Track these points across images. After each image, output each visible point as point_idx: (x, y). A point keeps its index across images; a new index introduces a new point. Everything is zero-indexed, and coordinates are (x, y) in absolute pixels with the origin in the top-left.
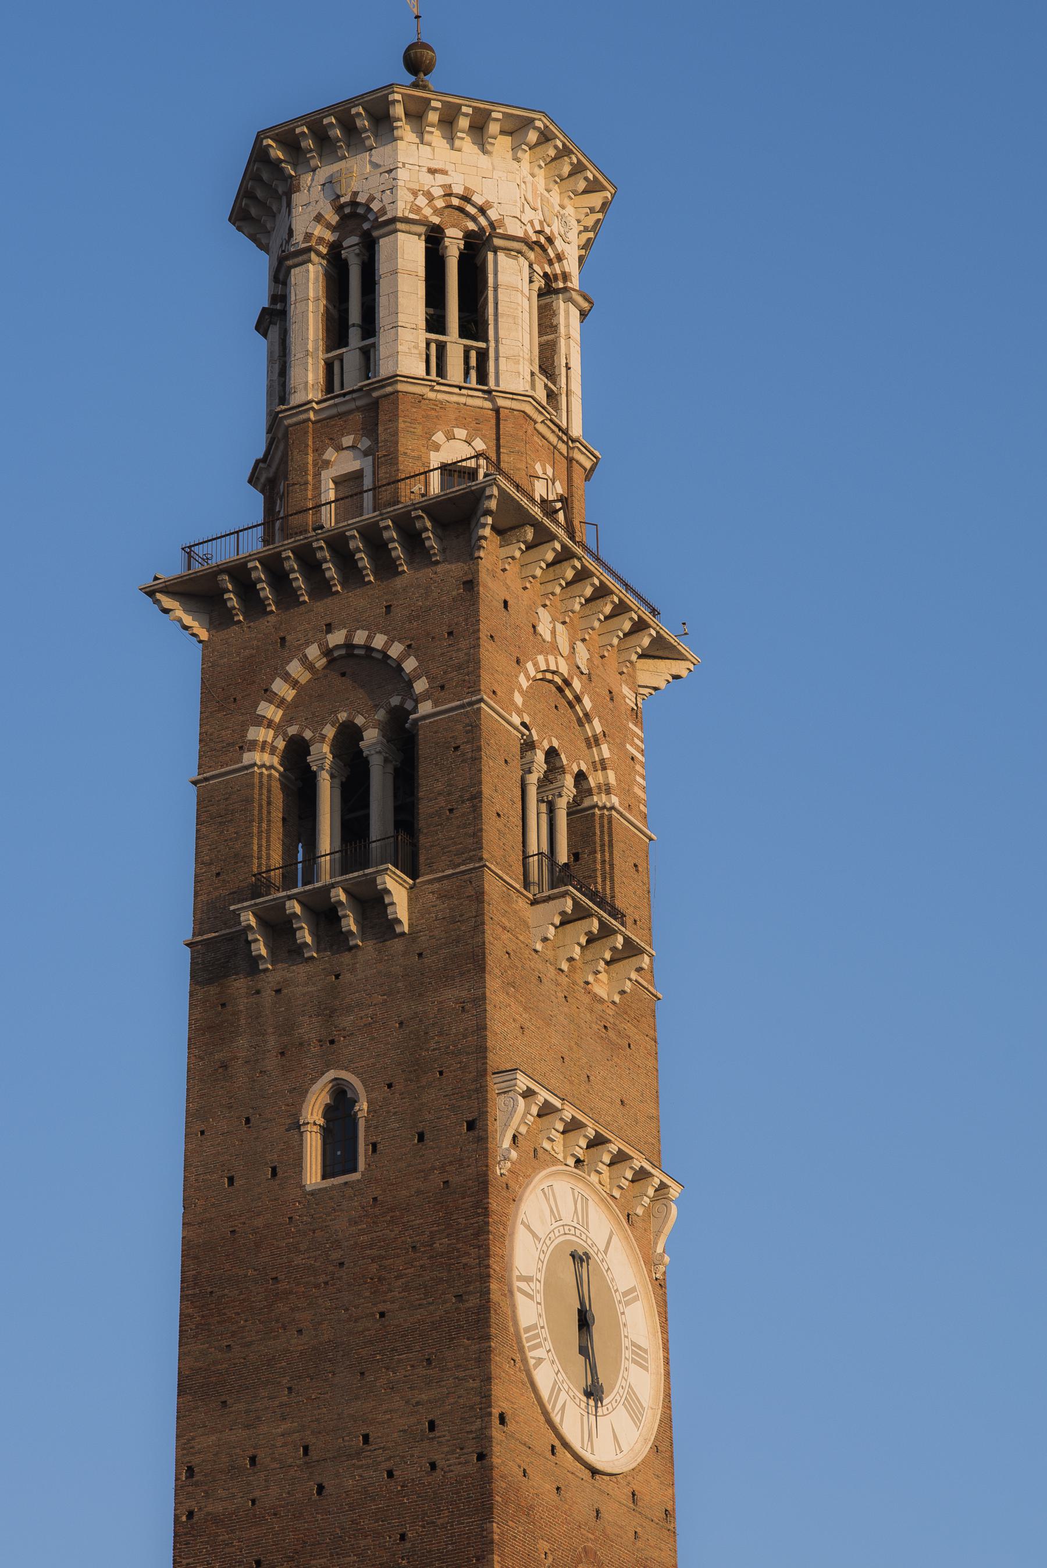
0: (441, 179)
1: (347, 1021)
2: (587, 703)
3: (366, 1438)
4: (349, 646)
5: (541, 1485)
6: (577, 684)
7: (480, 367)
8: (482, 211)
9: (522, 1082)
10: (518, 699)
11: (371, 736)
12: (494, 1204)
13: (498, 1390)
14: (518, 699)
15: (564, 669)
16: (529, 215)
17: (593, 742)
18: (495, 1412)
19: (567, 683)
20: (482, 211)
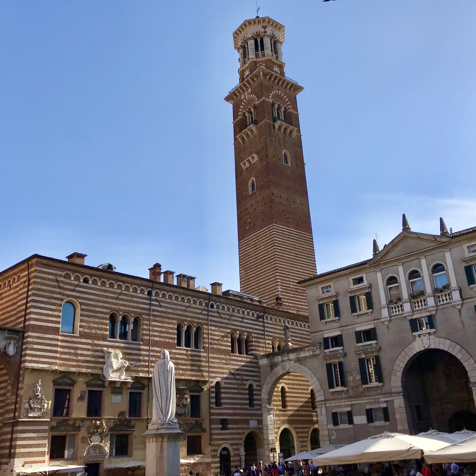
10: (270, 97)
11: (252, 108)
17: (287, 102)
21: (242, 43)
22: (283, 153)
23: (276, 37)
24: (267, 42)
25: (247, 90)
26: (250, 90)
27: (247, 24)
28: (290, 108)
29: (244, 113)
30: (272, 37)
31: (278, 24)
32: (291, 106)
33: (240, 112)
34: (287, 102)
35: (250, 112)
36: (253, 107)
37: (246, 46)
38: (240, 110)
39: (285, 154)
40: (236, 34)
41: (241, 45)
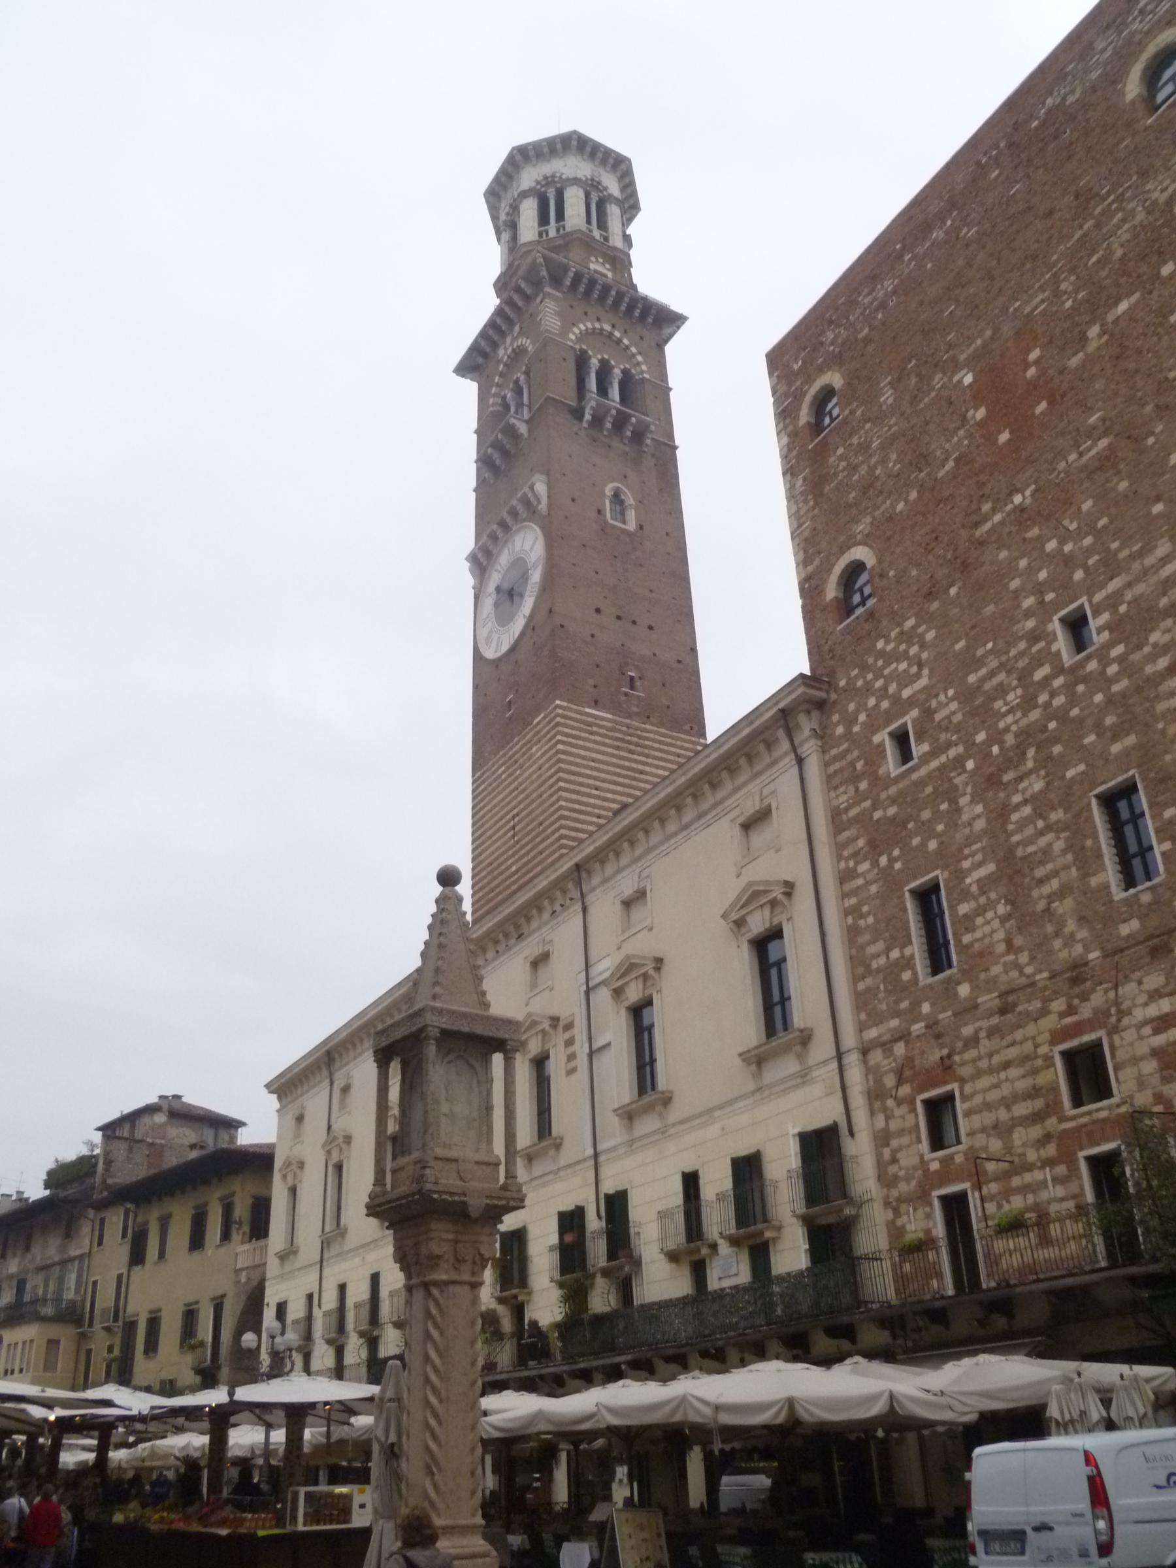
2: (626, 341)
4: (514, 350)
6: (617, 334)
11: (522, 378)
14: (572, 337)
17: (633, 356)
22: (608, 491)
24: (574, 201)
25: (511, 330)
26: (517, 328)
28: (642, 372)
29: (504, 397)
30: (591, 187)
31: (608, 152)
32: (644, 367)
33: (495, 395)
34: (633, 356)
35: (518, 391)
38: (494, 390)
39: (617, 497)
40: (494, 194)
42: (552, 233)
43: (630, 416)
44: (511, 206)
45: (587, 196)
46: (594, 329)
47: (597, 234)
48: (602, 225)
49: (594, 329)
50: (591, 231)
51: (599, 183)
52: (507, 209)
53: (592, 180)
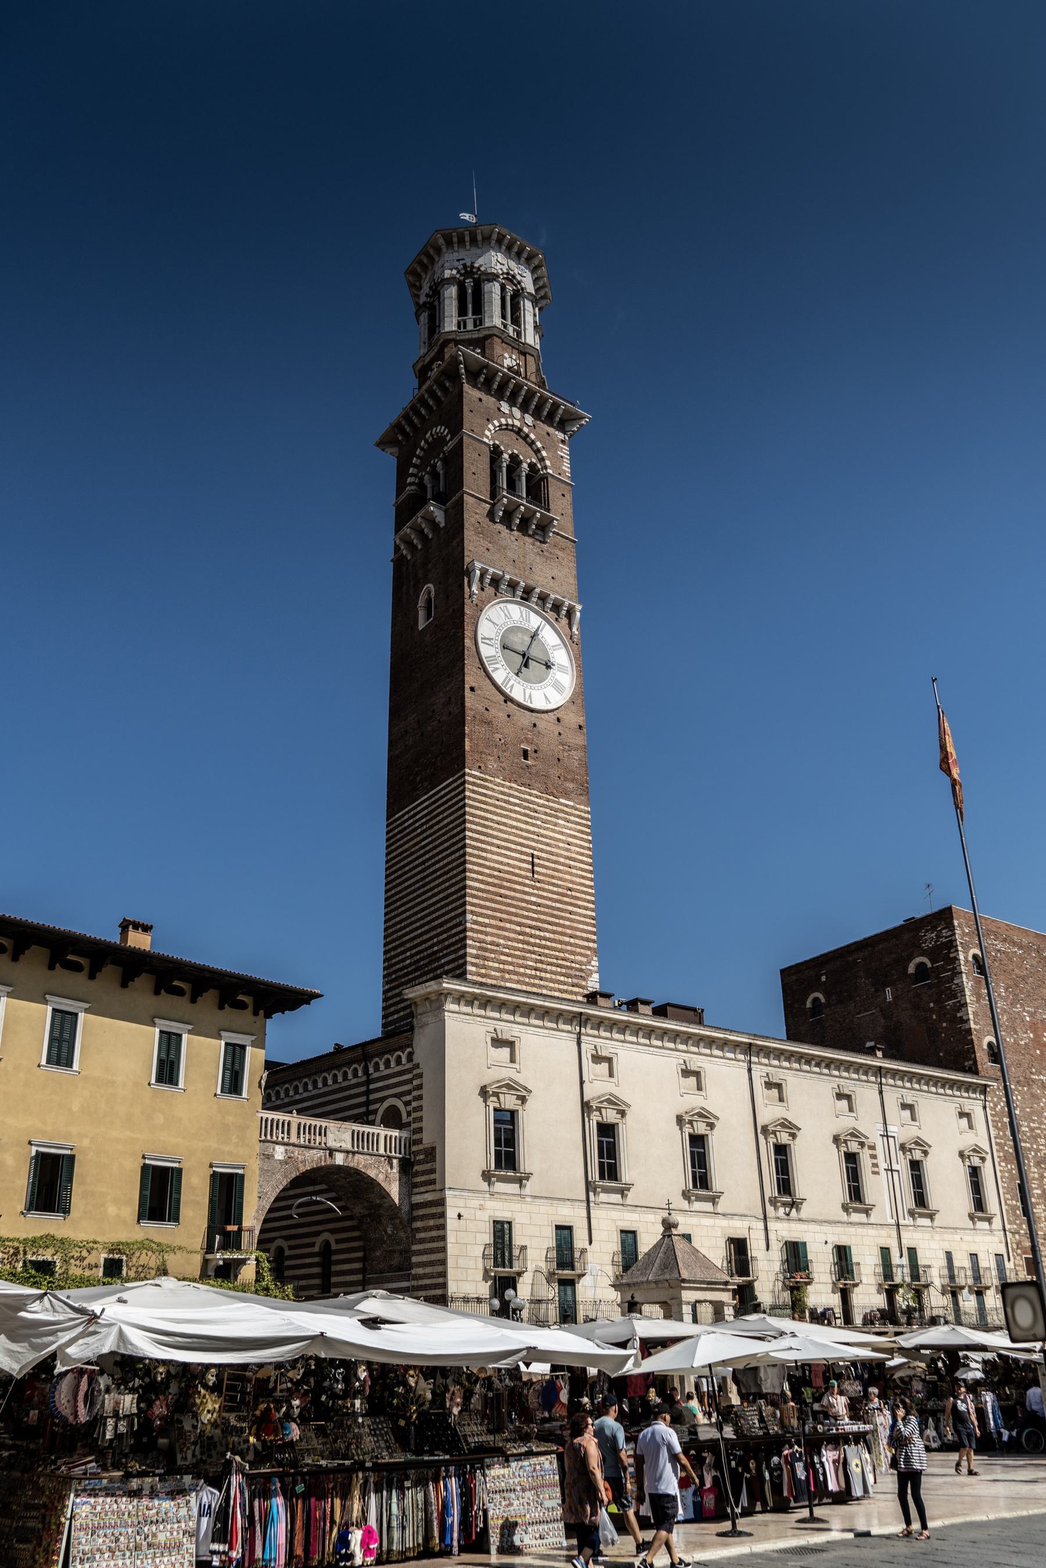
0: (462, 262)
1: (430, 566)
3: (433, 711)
5: (498, 713)
6: (526, 430)
7: (479, 323)
8: (479, 269)
9: (478, 565)
10: (487, 433)
12: (468, 611)
13: (466, 678)
15: (517, 423)
16: (499, 266)
18: (467, 686)
19: (520, 430)
20: (479, 269)
21: (427, 295)
23: (519, 283)
27: (441, 241)
29: (422, 479)
32: (548, 463)
35: (435, 475)
36: (441, 459)
37: (436, 303)
41: (425, 303)
42: (470, 326)
43: (535, 512)
44: (431, 288)
45: (503, 288)
46: (507, 425)
47: (511, 331)
48: (516, 321)
49: (507, 425)
50: (505, 326)
51: (514, 276)
52: (427, 290)
53: (508, 274)
